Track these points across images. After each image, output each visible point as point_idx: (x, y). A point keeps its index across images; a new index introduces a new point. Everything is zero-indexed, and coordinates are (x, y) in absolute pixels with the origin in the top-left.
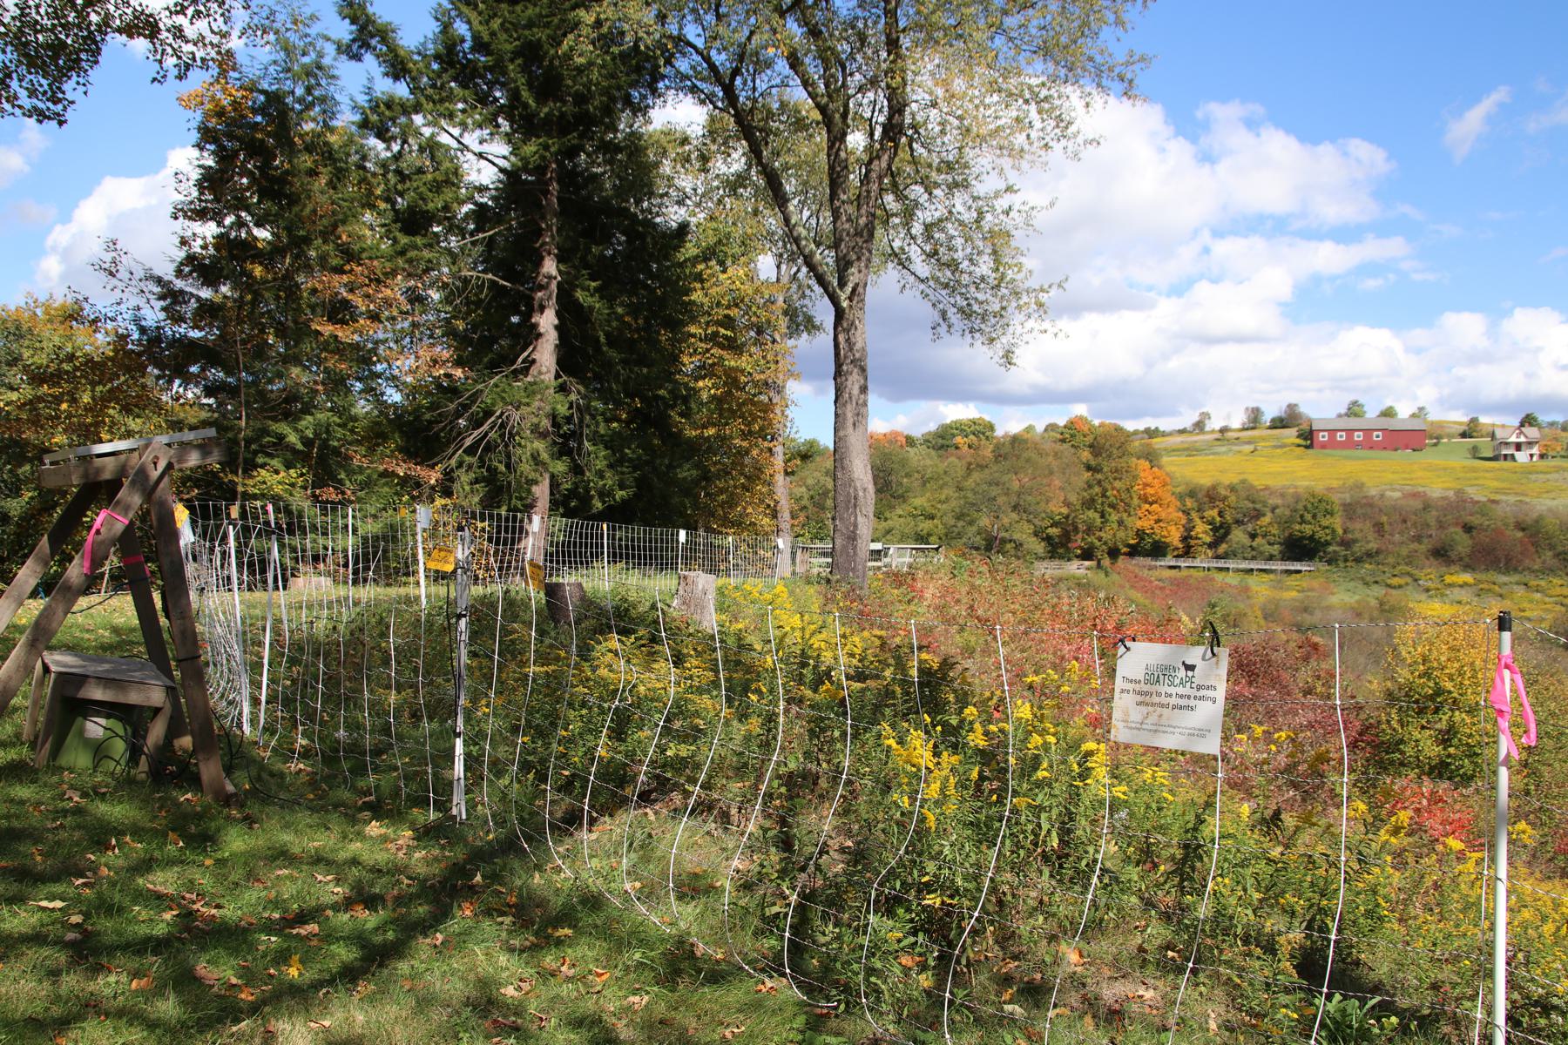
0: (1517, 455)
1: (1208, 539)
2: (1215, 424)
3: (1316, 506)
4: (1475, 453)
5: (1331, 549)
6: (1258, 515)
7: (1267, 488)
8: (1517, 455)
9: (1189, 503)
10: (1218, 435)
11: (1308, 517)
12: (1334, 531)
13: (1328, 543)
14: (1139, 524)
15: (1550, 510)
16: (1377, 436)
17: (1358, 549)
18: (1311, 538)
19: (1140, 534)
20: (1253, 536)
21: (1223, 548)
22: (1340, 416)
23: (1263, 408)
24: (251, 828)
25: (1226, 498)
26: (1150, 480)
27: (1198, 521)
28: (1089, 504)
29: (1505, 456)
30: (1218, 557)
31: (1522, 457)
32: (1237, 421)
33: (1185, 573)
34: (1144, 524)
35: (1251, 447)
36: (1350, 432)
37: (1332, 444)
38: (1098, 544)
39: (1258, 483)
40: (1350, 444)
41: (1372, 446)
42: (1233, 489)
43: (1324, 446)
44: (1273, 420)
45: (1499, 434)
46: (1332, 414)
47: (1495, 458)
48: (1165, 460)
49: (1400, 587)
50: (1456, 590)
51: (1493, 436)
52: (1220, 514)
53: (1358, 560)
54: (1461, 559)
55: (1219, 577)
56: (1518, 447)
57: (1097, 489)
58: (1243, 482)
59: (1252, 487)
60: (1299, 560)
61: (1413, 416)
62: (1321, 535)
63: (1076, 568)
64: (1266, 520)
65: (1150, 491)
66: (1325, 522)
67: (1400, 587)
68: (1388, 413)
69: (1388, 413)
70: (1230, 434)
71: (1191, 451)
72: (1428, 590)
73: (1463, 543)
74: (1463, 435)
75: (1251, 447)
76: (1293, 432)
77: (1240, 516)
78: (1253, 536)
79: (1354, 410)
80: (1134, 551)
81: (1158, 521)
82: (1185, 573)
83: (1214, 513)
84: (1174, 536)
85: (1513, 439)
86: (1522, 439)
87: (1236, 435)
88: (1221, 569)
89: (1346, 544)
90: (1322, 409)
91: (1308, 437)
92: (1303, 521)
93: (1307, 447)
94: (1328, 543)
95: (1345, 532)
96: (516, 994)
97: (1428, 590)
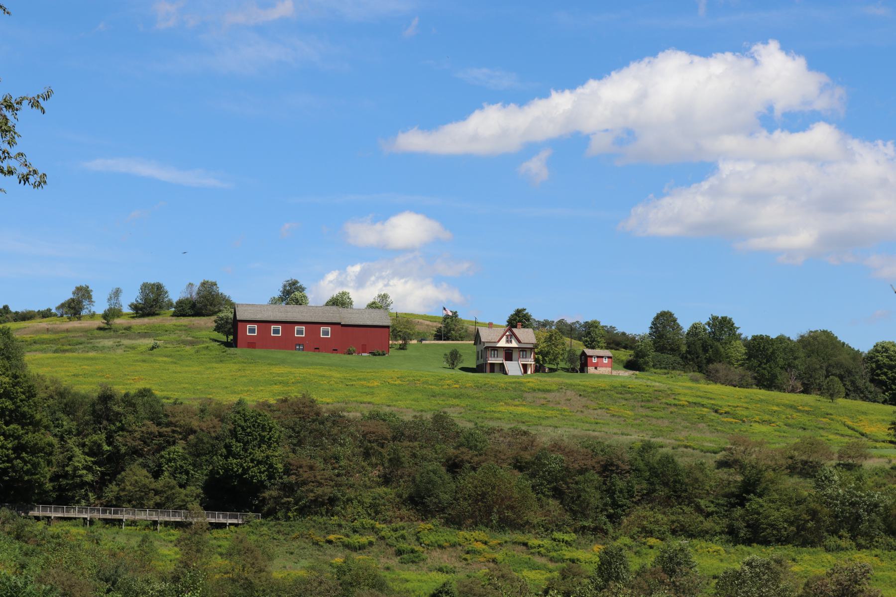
0: (508, 365)
2: (100, 306)
4: (453, 358)
8: (508, 365)
9: (67, 423)
10: (100, 322)
11: (237, 447)
12: (271, 466)
13: (262, 486)
15: (557, 446)
16: (325, 333)
17: (309, 493)
20: (157, 474)
21: (112, 490)
22: (274, 301)
23: (167, 287)
27: (77, 451)
29: (492, 365)
30: (108, 505)
31: (513, 368)
33: (54, 529)
35: (150, 342)
36: (289, 324)
37: (263, 342)
40: (287, 343)
41: (317, 346)
42: (128, 400)
43: (252, 344)
44: (180, 303)
45: (486, 336)
46: (266, 301)
47: (480, 369)
48: (28, 357)
49: (361, 548)
50: (437, 553)
51: (477, 338)
52: (110, 440)
53: (303, 511)
54: (443, 510)
55: (107, 534)
56: (509, 354)
58: (145, 393)
61: (372, 306)
66: (259, 455)
67: (361, 548)
68: (340, 302)
69: (340, 302)
70: (117, 322)
71: (63, 344)
72: (399, 553)
73: (445, 489)
74: (439, 336)
75: (150, 342)
76: (207, 323)
78: (157, 474)
79: (292, 293)
82: (54, 529)
85: (503, 343)
86: (514, 344)
88: (107, 521)
90: (251, 293)
91: (232, 331)
92: (230, 453)
93: (228, 344)
94: (262, 486)
97: (399, 553)
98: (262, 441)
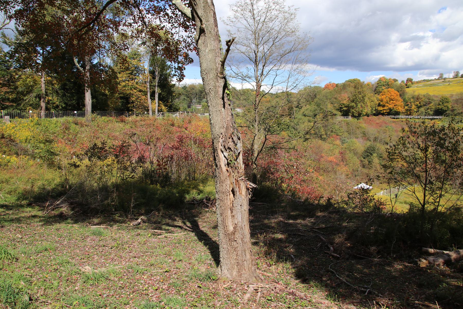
1: (416, 110)
3: (444, 100)
5: (447, 112)
6: (430, 103)
7: (434, 95)
11: (441, 103)
13: (446, 111)
14: (390, 106)
17: (456, 112)
18: (441, 109)
19: (390, 110)
24: (293, 195)
25: (422, 98)
26: (393, 94)
27: (413, 105)
28: (353, 101)
32: (451, 75)
34: (391, 106)
38: (355, 112)
39: (431, 94)
42: (424, 96)
52: (420, 103)
57: (354, 97)
59: (429, 95)
60: (438, 115)
62: (445, 109)
63: (350, 118)
64: (432, 104)
65: (392, 97)
75: (448, 84)
77: (425, 104)
80: (389, 114)
81: (395, 106)
83: (418, 103)
84: (401, 109)
87: (449, 80)
89: (453, 111)
92: (439, 105)
94: (446, 111)
95: (452, 107)
96: (340, 239)
98: (446, 102)
